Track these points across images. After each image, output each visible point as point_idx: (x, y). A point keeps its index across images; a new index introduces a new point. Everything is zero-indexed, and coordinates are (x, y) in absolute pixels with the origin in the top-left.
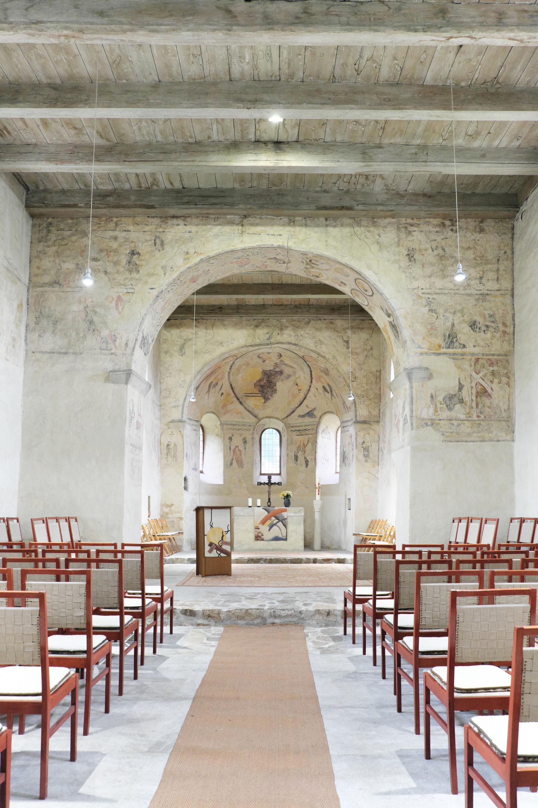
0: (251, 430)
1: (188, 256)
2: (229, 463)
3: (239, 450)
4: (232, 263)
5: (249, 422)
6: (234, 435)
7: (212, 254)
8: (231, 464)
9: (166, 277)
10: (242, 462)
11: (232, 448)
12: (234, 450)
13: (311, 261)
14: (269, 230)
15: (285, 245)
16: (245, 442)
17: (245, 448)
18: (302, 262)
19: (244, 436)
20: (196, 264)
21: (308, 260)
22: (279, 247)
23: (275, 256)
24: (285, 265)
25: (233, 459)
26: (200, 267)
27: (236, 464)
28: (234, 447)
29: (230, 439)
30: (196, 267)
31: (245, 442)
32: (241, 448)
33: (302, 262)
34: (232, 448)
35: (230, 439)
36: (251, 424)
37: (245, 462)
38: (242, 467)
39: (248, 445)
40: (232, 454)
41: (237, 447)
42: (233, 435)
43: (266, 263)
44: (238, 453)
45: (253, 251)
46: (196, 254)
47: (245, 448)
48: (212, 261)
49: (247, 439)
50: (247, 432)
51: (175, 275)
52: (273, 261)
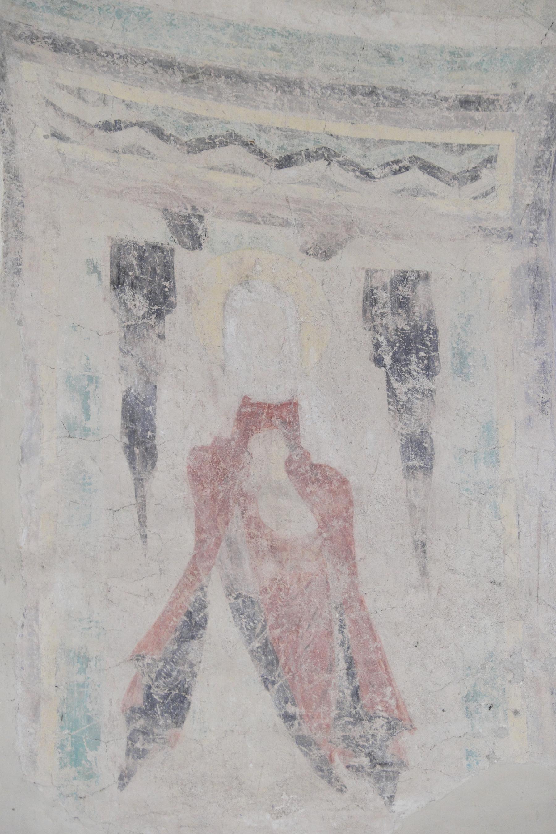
0: (502, 175)
2: (114, 690)
3: (309, 475)
5: (457, 59)
6: (219, 228)
8: (165, 702)
10: (366, 674)
11: (187, 424)
12: (217, 475)
16: (409, 347)
17: (418, 450)
19: (391, 260)
25: (193, 626)
27: (263, 706)
28: (219, 424)
29: (144, 280)
31: (409, 347)
32: (347, 427)
34: (187, 424)
35: (144, 280)
36: (495, 85)
37: (414, 675)
38: (384, 770)
39: (457, 410)
40: (179, 535)
41: (253, 416)
42: (189, 230)
44: (296, 519)
47: (418, 450)
49: (445, 307)
50: (448, 203)
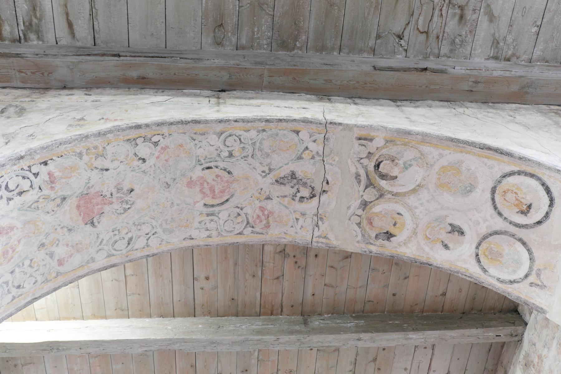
1: (82, 122)
4: (190, 184)
7: (142, 121)
9: (7, 146)
13: (377, 166)
14: (278, 102)
15: (320, 117)
18: (358, 176)
20: (100, 134)
21: (371, 168)
22: (306, 121)
23: (292, 167)
24: (315, 201)
26: (110, 149)
30: (99, 142)
33: (358, 176)
43: (269, 205)
45: (244, 135)
46: (102, 121)
48: (144, 150)
51: (34, 144)
52: (287, 190)
